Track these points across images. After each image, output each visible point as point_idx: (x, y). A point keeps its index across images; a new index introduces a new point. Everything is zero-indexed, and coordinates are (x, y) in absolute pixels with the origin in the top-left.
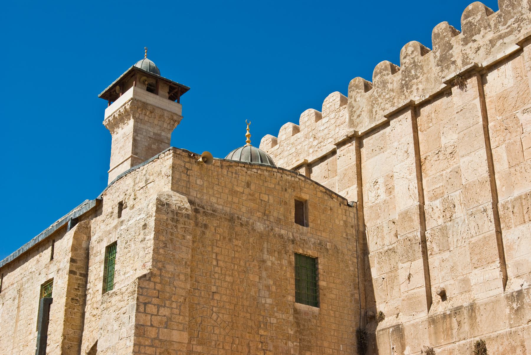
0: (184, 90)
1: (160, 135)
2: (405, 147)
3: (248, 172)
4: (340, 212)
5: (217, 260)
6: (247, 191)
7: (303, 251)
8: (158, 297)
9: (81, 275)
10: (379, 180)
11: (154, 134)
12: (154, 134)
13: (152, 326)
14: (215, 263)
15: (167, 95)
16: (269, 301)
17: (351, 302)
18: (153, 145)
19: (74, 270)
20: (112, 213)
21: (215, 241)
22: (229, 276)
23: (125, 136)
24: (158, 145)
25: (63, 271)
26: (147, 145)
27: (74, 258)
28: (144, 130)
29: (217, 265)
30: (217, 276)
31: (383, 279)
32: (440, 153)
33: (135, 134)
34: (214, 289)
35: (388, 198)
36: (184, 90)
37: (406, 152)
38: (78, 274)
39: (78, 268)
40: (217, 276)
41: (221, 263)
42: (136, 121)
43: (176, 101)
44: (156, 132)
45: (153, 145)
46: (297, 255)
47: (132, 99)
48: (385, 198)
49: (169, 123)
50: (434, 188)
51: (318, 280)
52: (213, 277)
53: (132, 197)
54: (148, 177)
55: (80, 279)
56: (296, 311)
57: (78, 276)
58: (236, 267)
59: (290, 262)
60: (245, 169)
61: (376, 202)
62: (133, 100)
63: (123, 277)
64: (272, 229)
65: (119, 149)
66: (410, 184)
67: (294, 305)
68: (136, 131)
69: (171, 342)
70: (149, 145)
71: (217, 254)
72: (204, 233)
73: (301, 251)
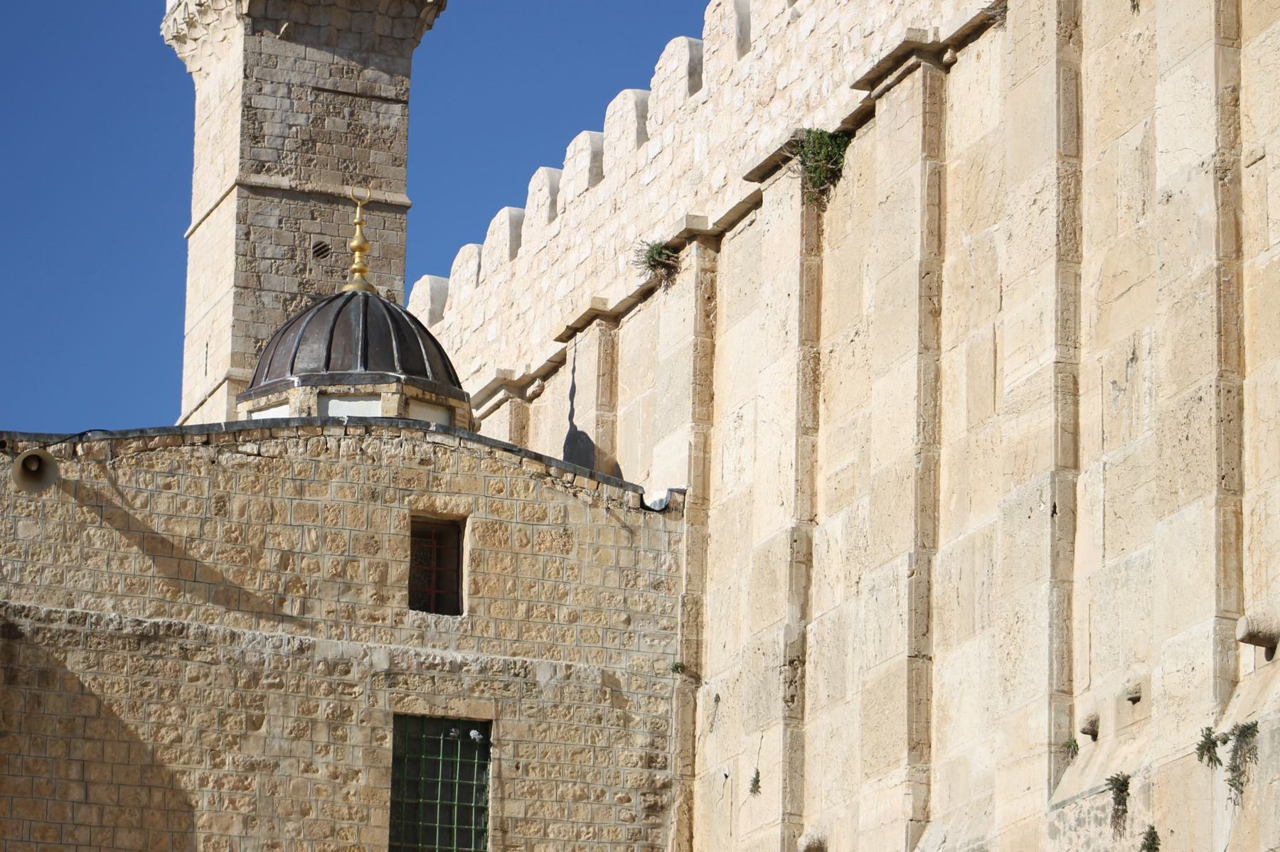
3: (225, 458)
5: (86, 784)
7: (432, 705)
14: (76, 793)
21: (79, 721)
22: (131, 828)
29: (86, 801)
30: (82, 835)
33: (252, 89)
40: (82, 835)
41: (99, 793)
46: (403, 722)
49: (398, 16)
52: (70, 840)
58: (157, 796)
71: (84, 764)
72: (38, 701)
73: (420, 708)
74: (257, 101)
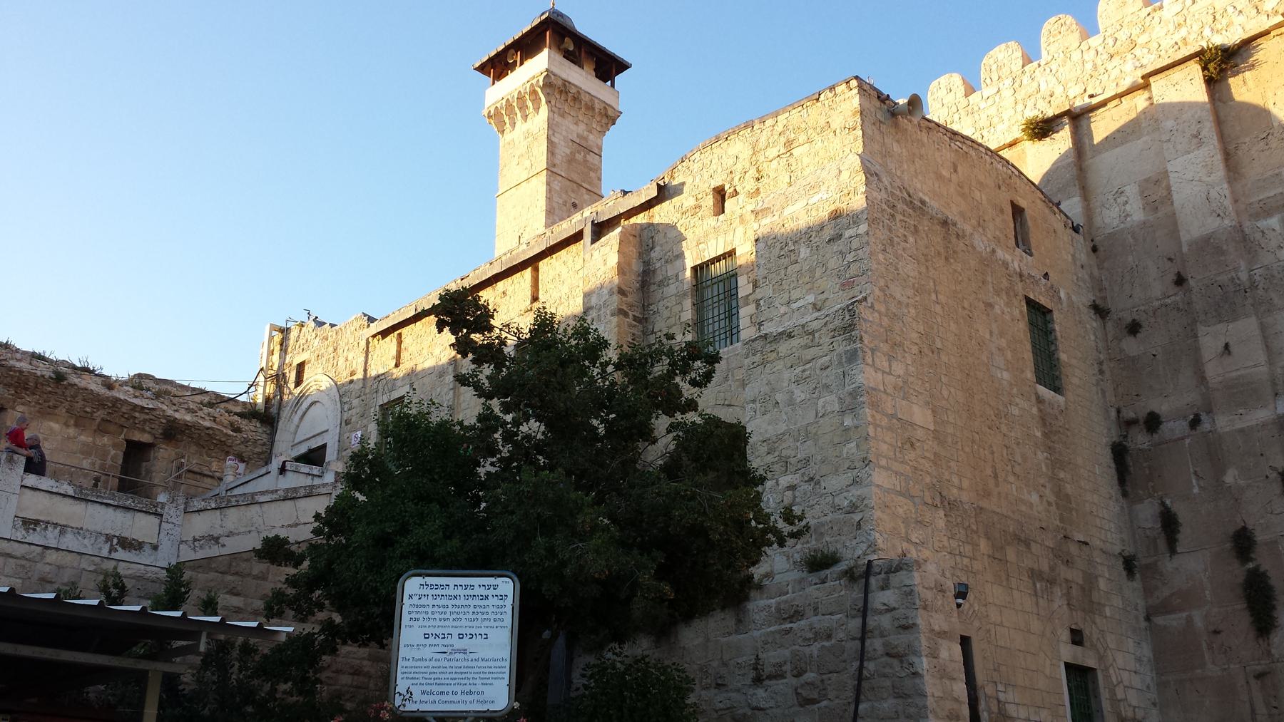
0: (622, 66)
1: (586, 139)
2: (1192, 127)
4: (1066, 239)
5: (936, 292)
6: (954, 177)
8: (887, 342)
9: (635, 318)
10: (1127, 189)
11: (578, 136)
12: (578, 136)
13: (885, 392)
14: (933, 297)
15: (594, 73)
16: (1006, 375)
17: (1097, 393)
18: (577, 155)
19: (624, 308)
20: (698, 207)
23: (527, 135)
24: (585, 156)
25: (600, 310)
26: (568, 153)
27: (624, 287)
28: (564, 128)
31: (1154, 355)
32: (1270, 137)
33: (551, 133)
34: (939, 344)
35: (1151, 218)
36: (622, 66)
37: (1196, 137)
38: (631, 316)
39: (631, 306)
42: (551, 111)
43: (609, 83)
44: (581, 132)
45: (577, 155)
47: (547, 70)
48: (1142, 218)
49: (600, 122)
50: (1261, 197)
51: (1057, 350)
53: (753, 172)
54: (793, 135)
55: (634, 326)
56: (1040, 400)
57: (630, 320)
59: (1021, 312)
60: (948, 139)
61: (1122, 225)
62: (549, 74)
63: (783, 309)
64: (994, 251)
65: (517, 157)
66: (1211, 191)
67: (1035, 389)
68: (551, 126)
69: (912, 424)
70: (571, 153)
73: (1032, 297)
74: (553, 139)
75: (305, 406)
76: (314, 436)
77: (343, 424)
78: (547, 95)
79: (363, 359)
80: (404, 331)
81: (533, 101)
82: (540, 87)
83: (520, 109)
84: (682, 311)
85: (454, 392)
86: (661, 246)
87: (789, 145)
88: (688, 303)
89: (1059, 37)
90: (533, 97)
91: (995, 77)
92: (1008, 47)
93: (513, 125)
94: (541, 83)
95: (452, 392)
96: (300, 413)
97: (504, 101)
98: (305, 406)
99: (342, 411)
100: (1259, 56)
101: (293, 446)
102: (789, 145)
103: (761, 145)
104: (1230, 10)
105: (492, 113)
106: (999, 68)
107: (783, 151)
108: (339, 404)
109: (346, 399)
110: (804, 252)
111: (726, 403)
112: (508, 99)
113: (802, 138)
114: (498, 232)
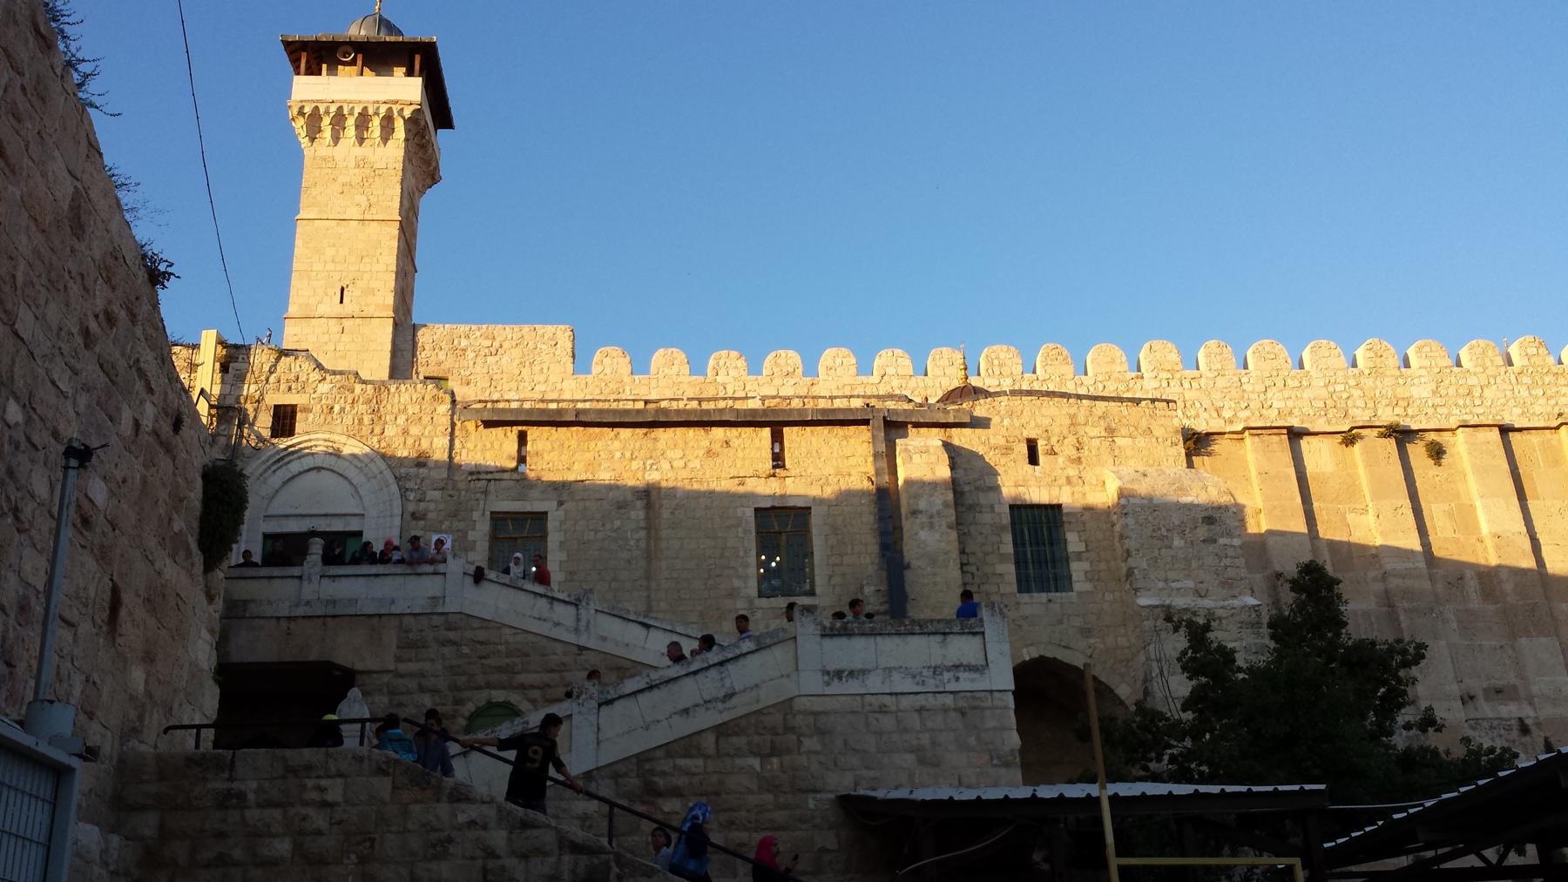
23: (361, 163)
53: (1071, 439)
75: (295, 467)
76: (326, 515)
77: (407, 517)
78: (407, 131)
79: (446, 441)
80: (533, 433)
81: (382, 127)
82: (403, 118)
83: (357, 127)
84: (1001, 542)
85: (648, 533)
86: (965, 470)
87: (1111, 431)
88: (1008, 538)
89: (1056, 362)
90: (385, 123)
91: (997, 372)
92: (1008, 350)
93: (336, 139)
94: (407, 113)
95: (642, 534)
96: (282, 474)
97: (333, 109)
98: (295, 467)
99: (403, 496)
100: (1215, 447)
101: (265, 516)
102: (1111, 431)
103: (1081, 419)
104: (1198, 405)
105: (308, 110)
106: (1000, 365)
107: (1103, 434)
108: (394, 488)
109: (409, 485)
110: (1177, 542)
111: (1063, 644)
112: (341, 108)
113: (1124, 431)
114: (296, 266)
